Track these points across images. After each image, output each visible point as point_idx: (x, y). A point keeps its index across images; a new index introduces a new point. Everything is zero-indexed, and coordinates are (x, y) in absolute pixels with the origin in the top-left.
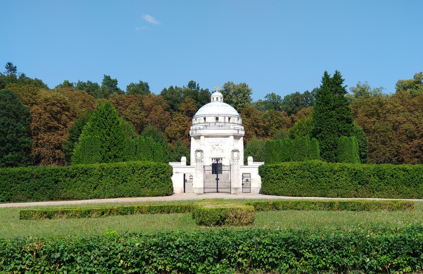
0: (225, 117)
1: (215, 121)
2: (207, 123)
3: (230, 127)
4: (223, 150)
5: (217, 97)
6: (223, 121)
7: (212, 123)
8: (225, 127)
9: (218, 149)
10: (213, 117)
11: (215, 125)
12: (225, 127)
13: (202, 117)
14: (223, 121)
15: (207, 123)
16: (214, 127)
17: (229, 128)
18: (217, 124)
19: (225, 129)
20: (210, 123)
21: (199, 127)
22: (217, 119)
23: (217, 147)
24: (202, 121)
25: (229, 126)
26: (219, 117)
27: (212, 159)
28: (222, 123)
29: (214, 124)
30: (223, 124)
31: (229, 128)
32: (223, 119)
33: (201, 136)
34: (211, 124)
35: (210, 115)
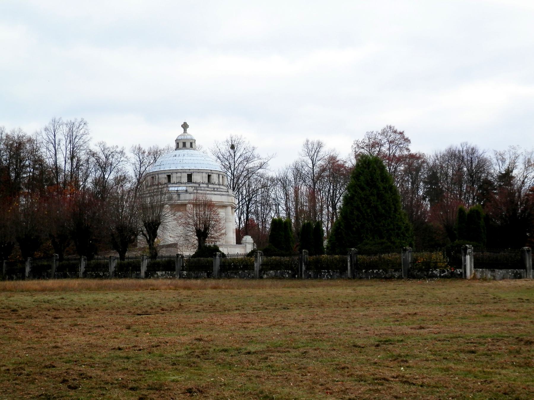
2: (196, 183)
5: (191, 141)
6: (217, 182)
8: (221, 191)
11: (208, 187)
12: (221, 191)
13: (186, 172)
14: (217, 182)
15: (196, 183)
17: (227, 193)
18: (210, 186)
19: (223, 195)
20: (199, 184)
21: (185, 188)
22: (190, 177)
24: (185, 179)
25: (227, 190)
26: (212, 174)
28: (216, 185)
29: (205, 186)
30: (217, 186)
34: (201, 185)
35: (199, 171)
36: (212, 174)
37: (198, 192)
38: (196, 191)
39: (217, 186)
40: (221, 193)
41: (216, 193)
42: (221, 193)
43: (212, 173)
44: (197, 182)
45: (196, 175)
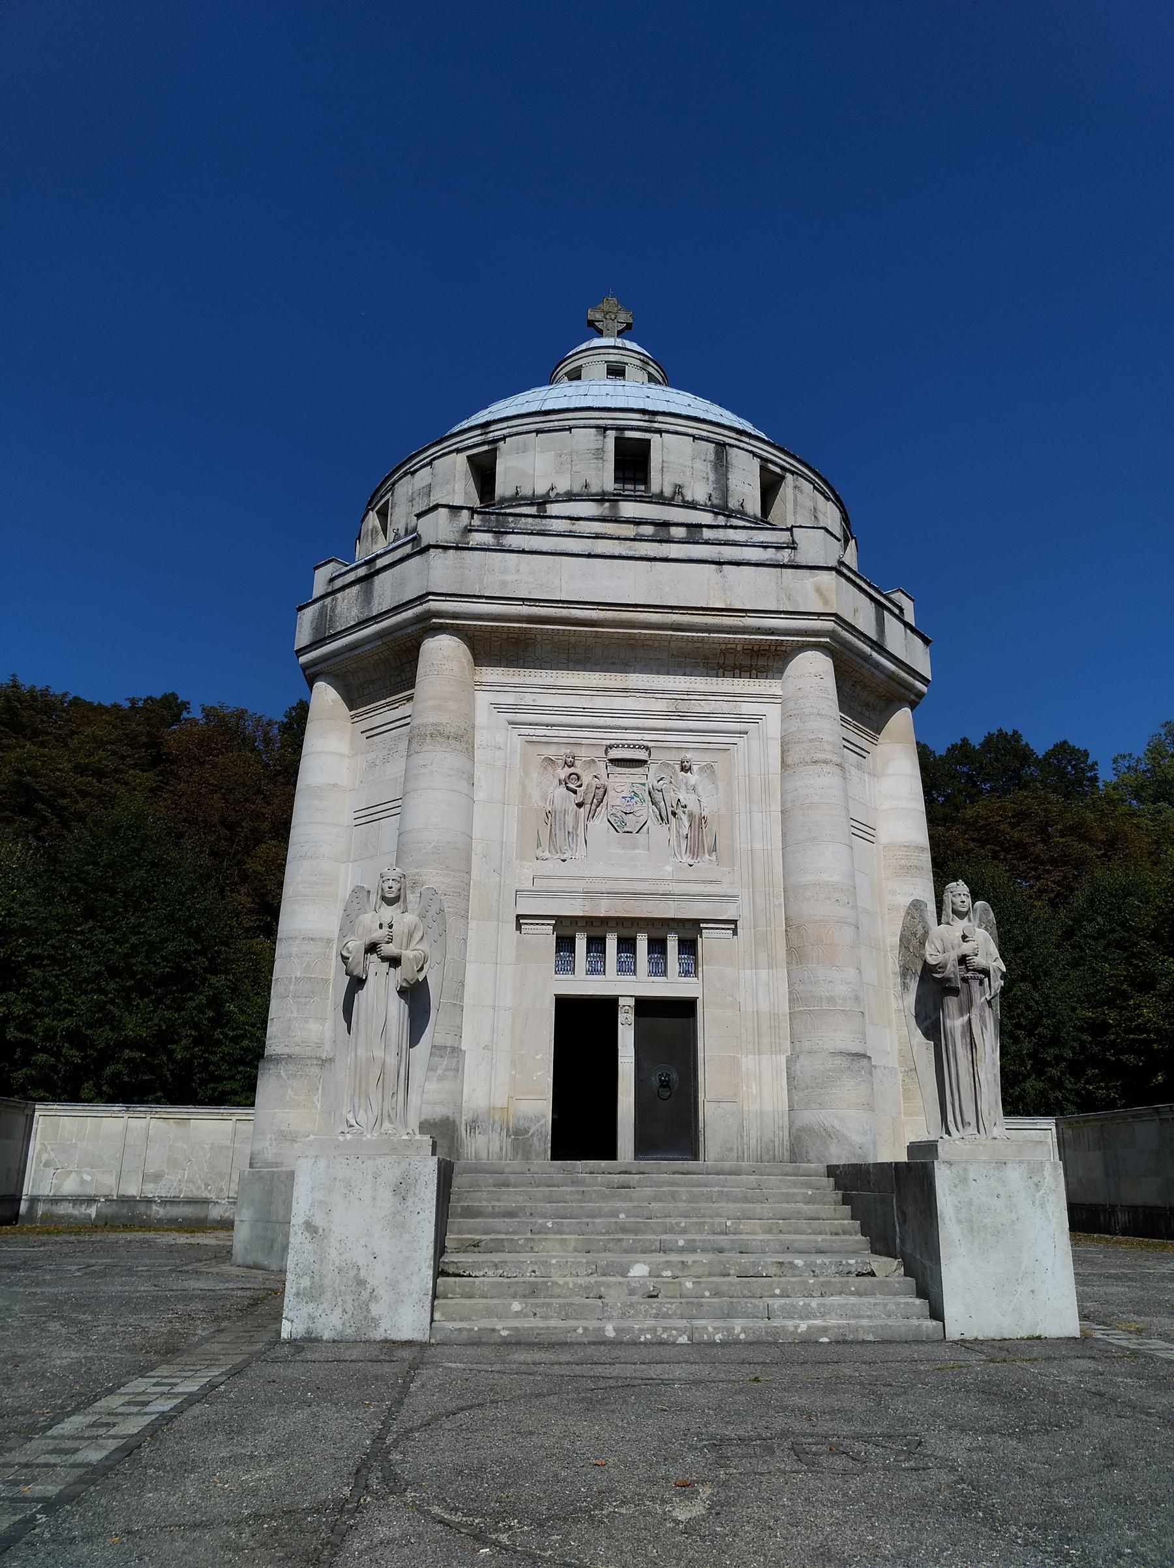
0: (721, 446)
1: (605, 478)
3: (793, 546)
4: (699, 822)
6: (699, 491)
7: (570, 497)
8: (735, 544)
9: (646, 811)
10: (585, 438)
16: (598, 537)
17: (785, 556)
18: (629, 509)
23: (622, 782)
25: (784, 537)
26: (655, 438)
27: (565, 944)
28: (692, 506)
30: (706, 518)
31: (785, 556)
32: (704, 468)
33: (427, 626)
36: (655, 438)
37: (512, 541)
38: (487, 538)
39: (706, 518)
40: (729, 553)
41: (674, 550)
42: (729, 553)
43: (660, 432)
44: (526, 491)
45: (525, 449)
